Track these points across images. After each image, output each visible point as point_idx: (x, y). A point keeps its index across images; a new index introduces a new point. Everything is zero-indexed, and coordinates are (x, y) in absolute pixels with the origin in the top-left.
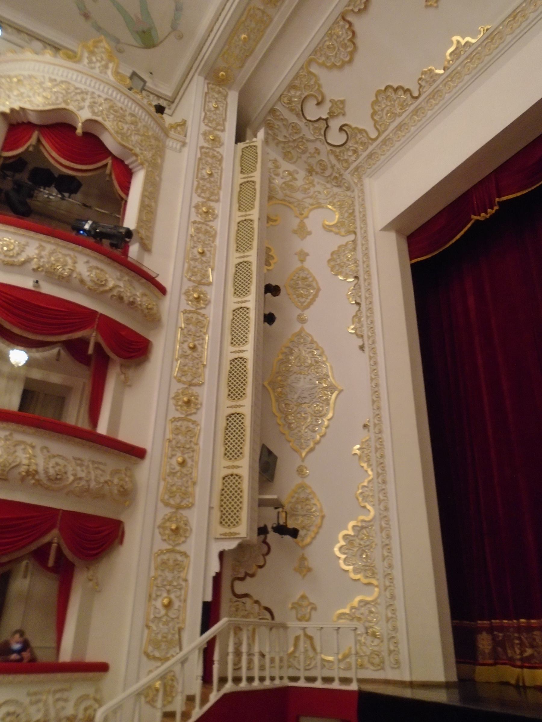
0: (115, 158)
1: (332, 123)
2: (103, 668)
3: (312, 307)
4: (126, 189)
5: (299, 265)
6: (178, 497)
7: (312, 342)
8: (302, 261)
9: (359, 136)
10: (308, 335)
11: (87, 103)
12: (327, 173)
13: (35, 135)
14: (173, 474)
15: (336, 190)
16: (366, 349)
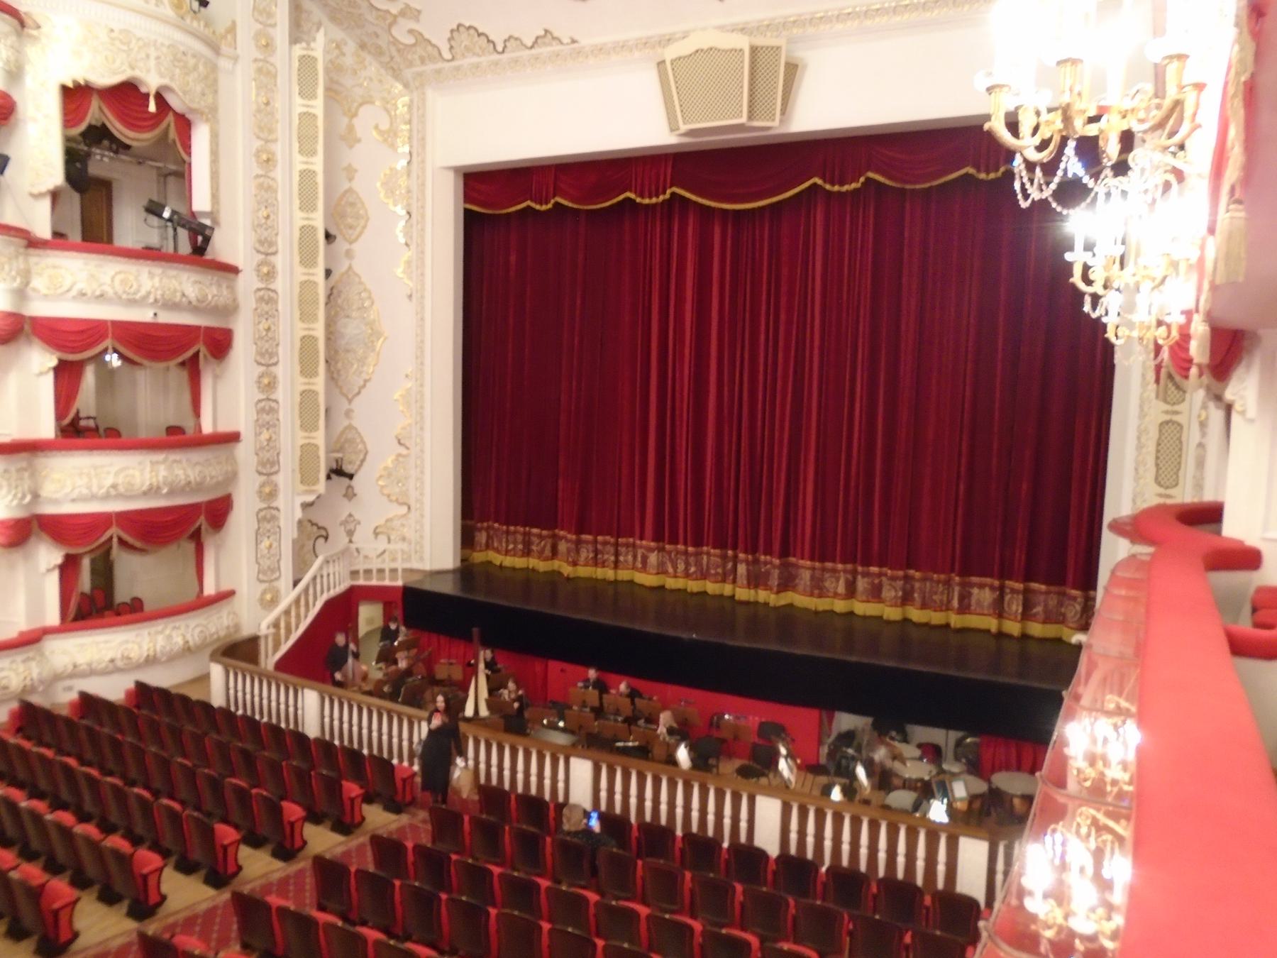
0: (176, 114)
1: (400, 20)
2: (230, 594)
3: (360, 240)
4: (187, 148)
5: (346, 186)
6: (268, 467)
7: (361, 283)
8: (350, 180)
9: (430, 48)
10: (357, 275)
11: (152, 63)
12: (386, 59)
13: (95, 103)
14: (262, 448)
15: (389, 79)
16: (414, 299)
